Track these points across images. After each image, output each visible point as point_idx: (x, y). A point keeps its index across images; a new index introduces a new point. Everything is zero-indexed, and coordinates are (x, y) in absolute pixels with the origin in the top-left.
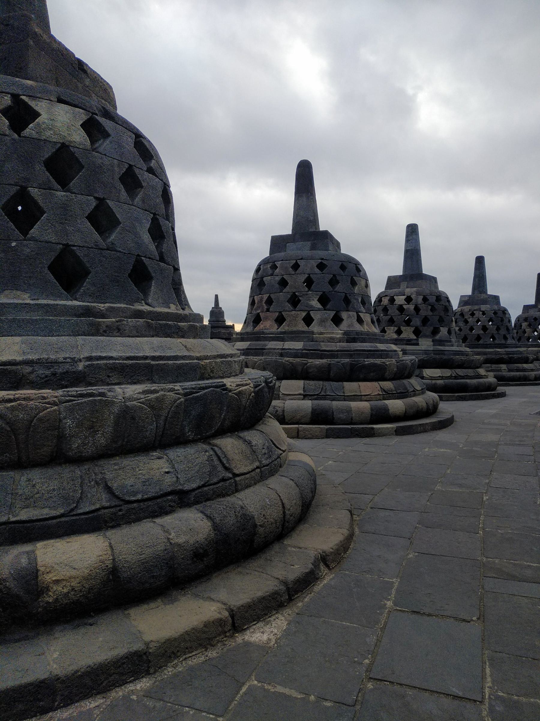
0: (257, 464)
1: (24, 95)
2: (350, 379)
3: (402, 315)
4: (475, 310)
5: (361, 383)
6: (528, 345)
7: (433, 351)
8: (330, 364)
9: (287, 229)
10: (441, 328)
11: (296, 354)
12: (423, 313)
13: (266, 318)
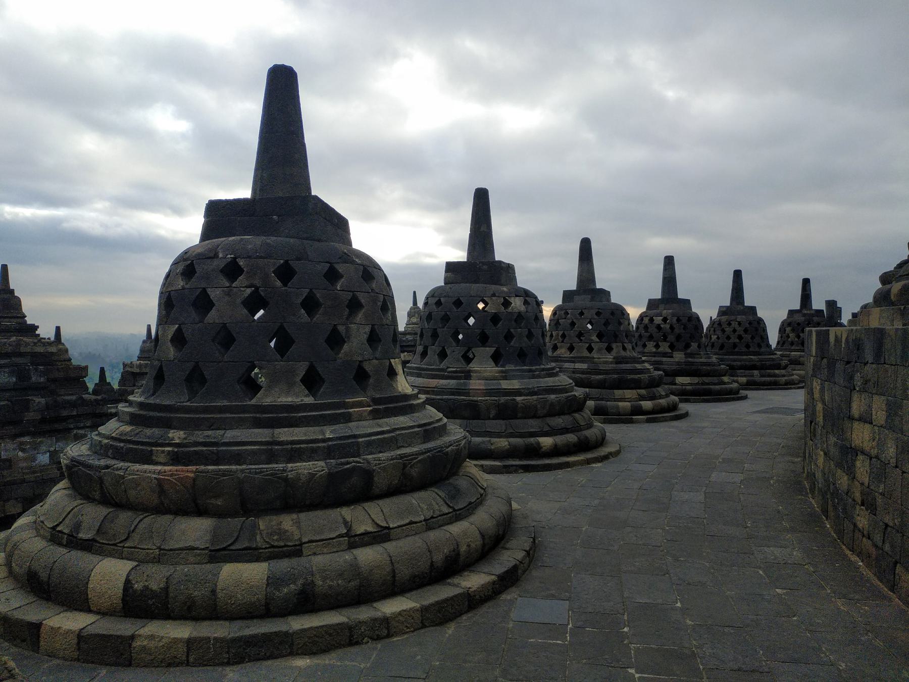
3: (659, 332)
4: (731, 321)
5: (624, 391)
7: (684, 362)
9: (573, 286)
10: (692, 343)
11: (583, 372)
12: (677, 331)
13: (561, 347)
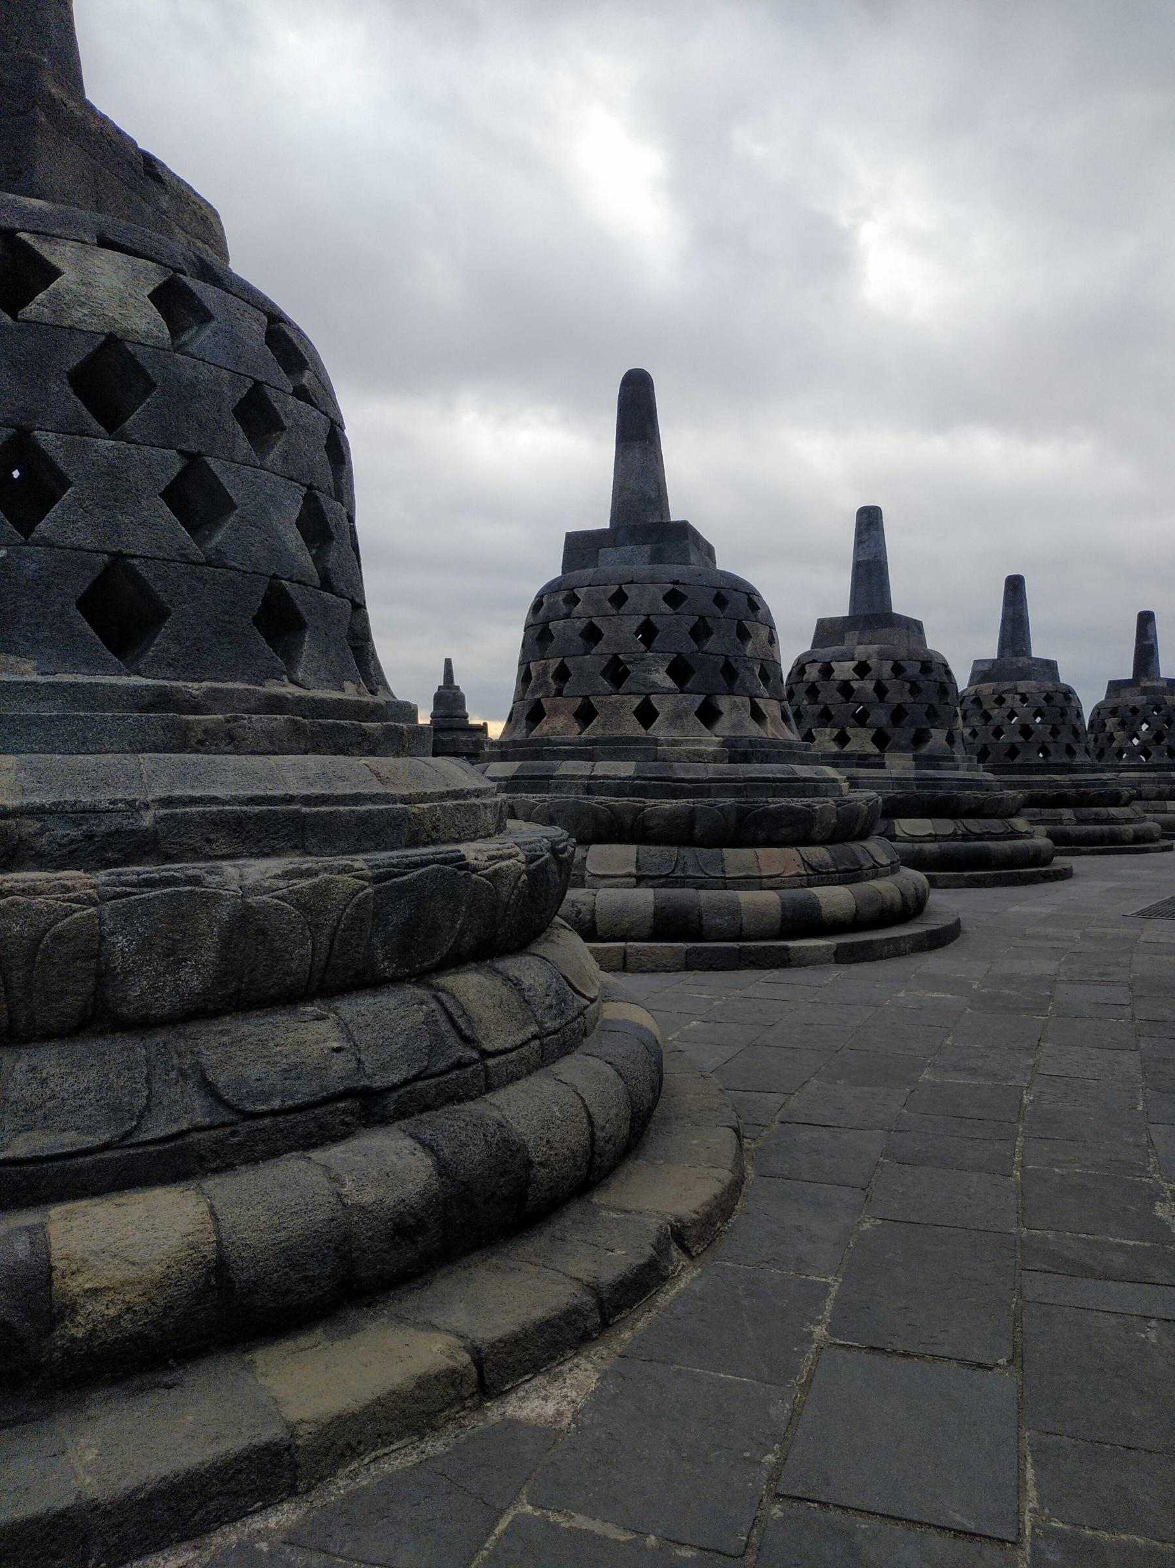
0: (533, 1029)
1: (25, 231)
2: (738, 842)
4: (1005, 692)
5: (760, 851)
6: (1117, 766)
7: (915, 779)
8: (694, 808)
9: (600, 519)
10: (933, 731)
11: (621, 788)
13: (556, 711)
